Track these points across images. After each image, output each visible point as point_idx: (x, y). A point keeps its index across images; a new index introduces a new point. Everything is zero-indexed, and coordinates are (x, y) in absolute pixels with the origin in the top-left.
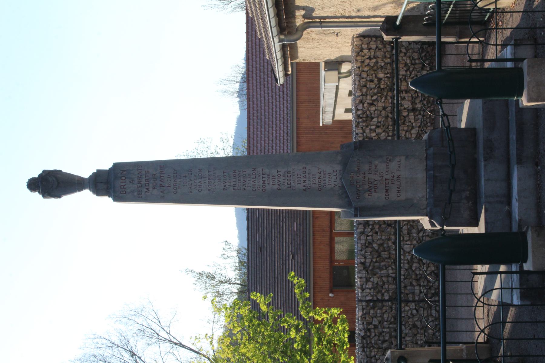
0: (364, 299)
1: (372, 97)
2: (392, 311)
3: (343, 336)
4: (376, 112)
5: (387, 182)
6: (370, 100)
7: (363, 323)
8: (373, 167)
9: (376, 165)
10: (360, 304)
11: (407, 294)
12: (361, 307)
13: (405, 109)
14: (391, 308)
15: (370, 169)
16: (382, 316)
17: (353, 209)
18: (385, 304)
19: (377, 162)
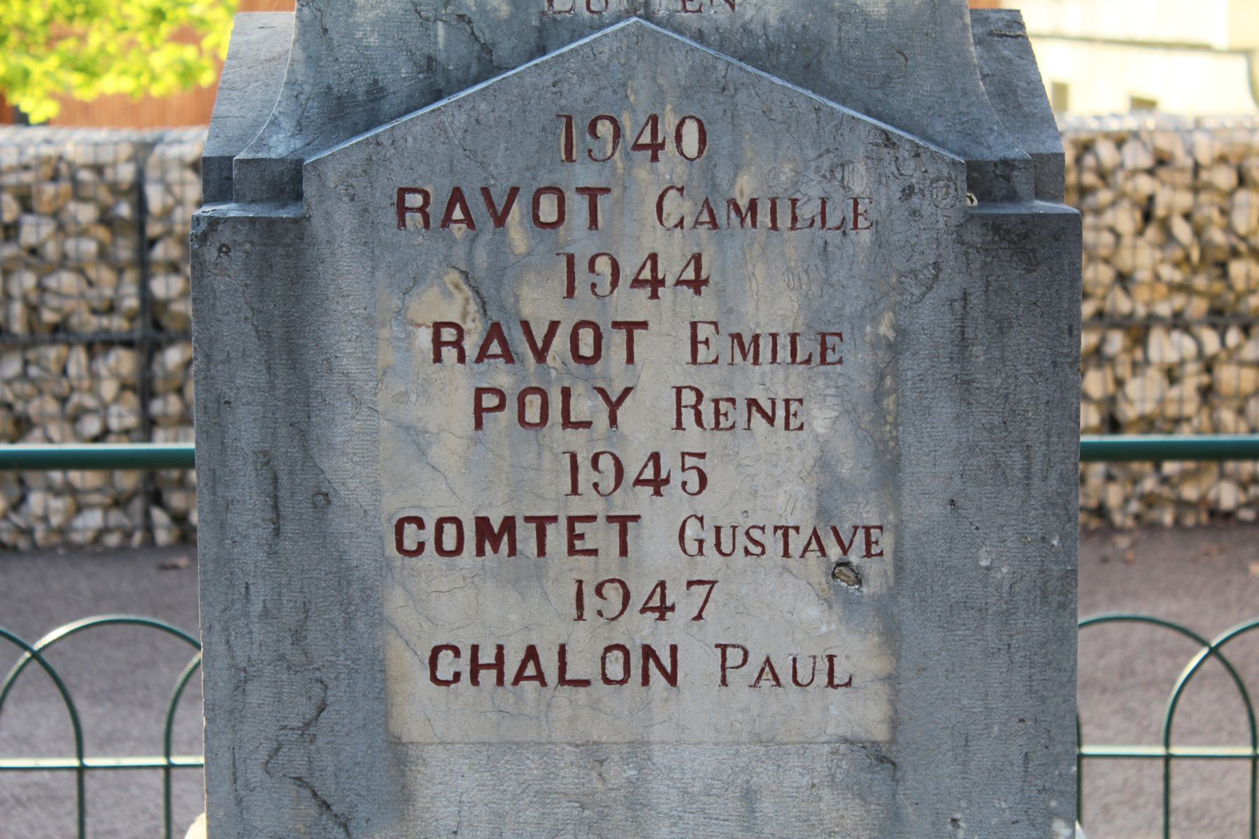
0: (152, 173)
1: (1187, 216)
2: (95, 312)
3: (123, 72)
4: (1107, 238)
5: (601, 536)
6: (1170, 209)
7: (26, 168)
8: (768, 381)
9: (787, 415)
10: (125, 151)
11: (180, 391)
12: (106, 156)
13: (1120, 383)
14: (111, 308)
15: (747, 346)
16: (64, 262)
17: (281, 146)
18: (130, 277)
19: (820, 419)
